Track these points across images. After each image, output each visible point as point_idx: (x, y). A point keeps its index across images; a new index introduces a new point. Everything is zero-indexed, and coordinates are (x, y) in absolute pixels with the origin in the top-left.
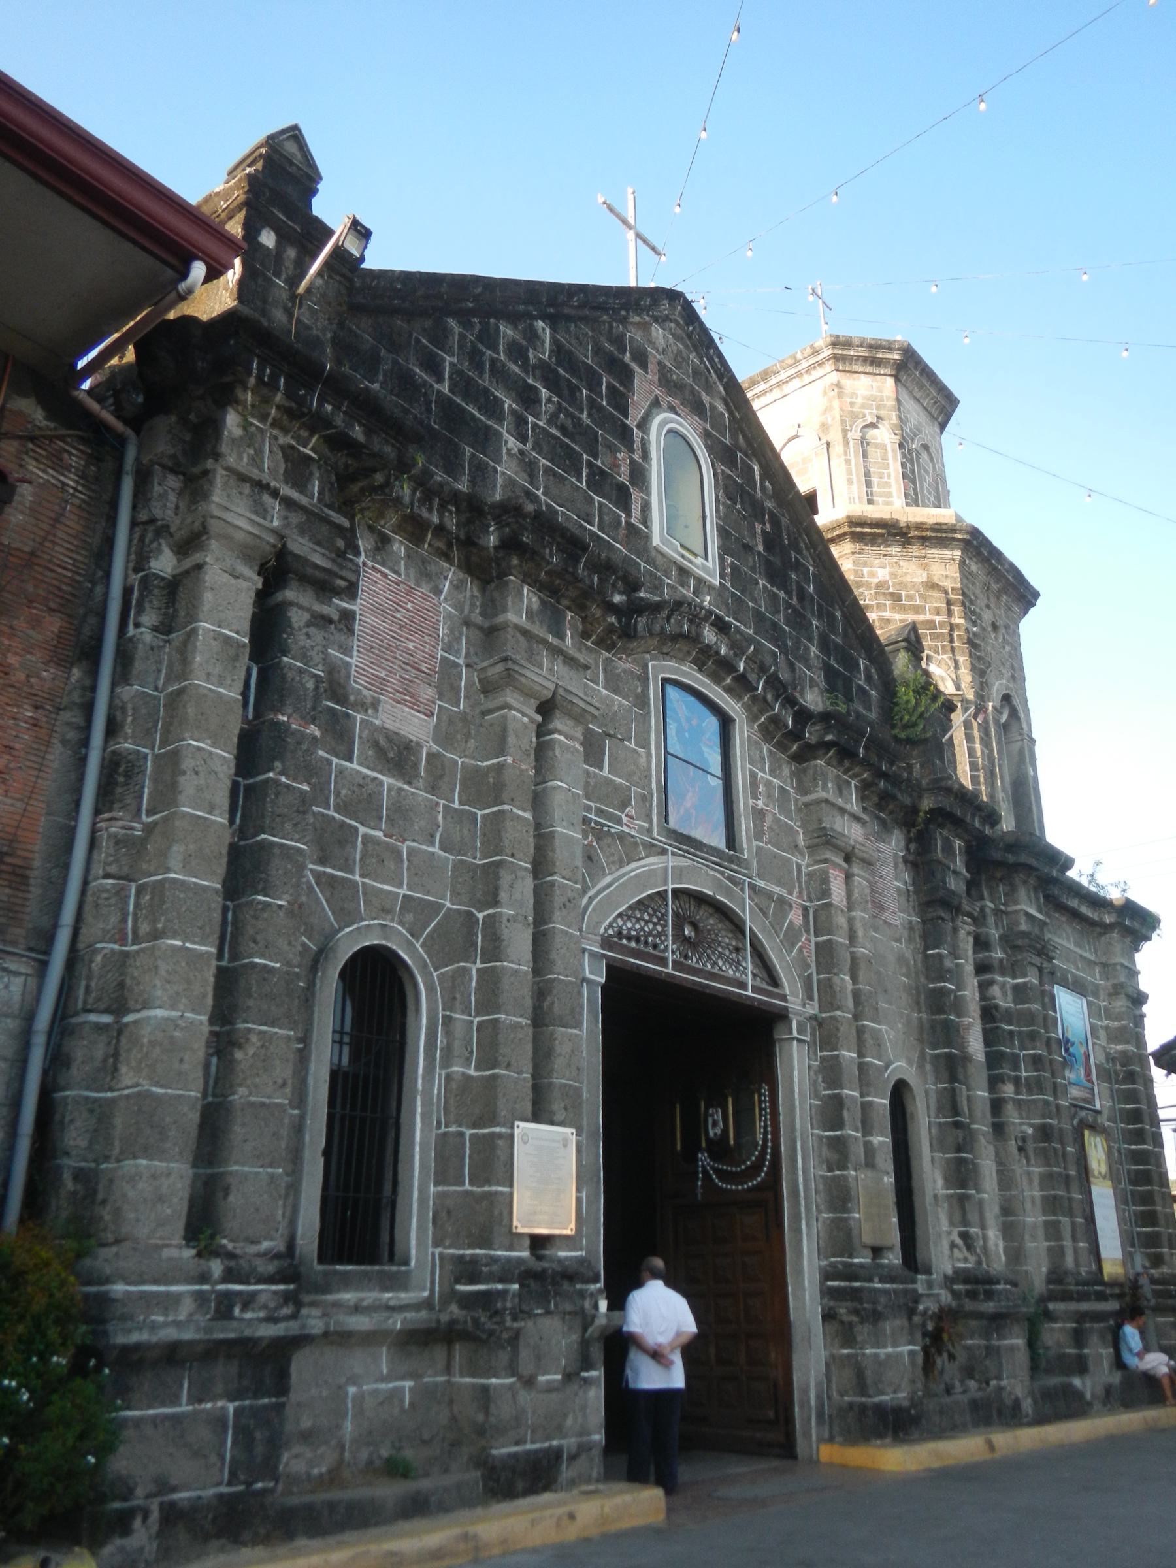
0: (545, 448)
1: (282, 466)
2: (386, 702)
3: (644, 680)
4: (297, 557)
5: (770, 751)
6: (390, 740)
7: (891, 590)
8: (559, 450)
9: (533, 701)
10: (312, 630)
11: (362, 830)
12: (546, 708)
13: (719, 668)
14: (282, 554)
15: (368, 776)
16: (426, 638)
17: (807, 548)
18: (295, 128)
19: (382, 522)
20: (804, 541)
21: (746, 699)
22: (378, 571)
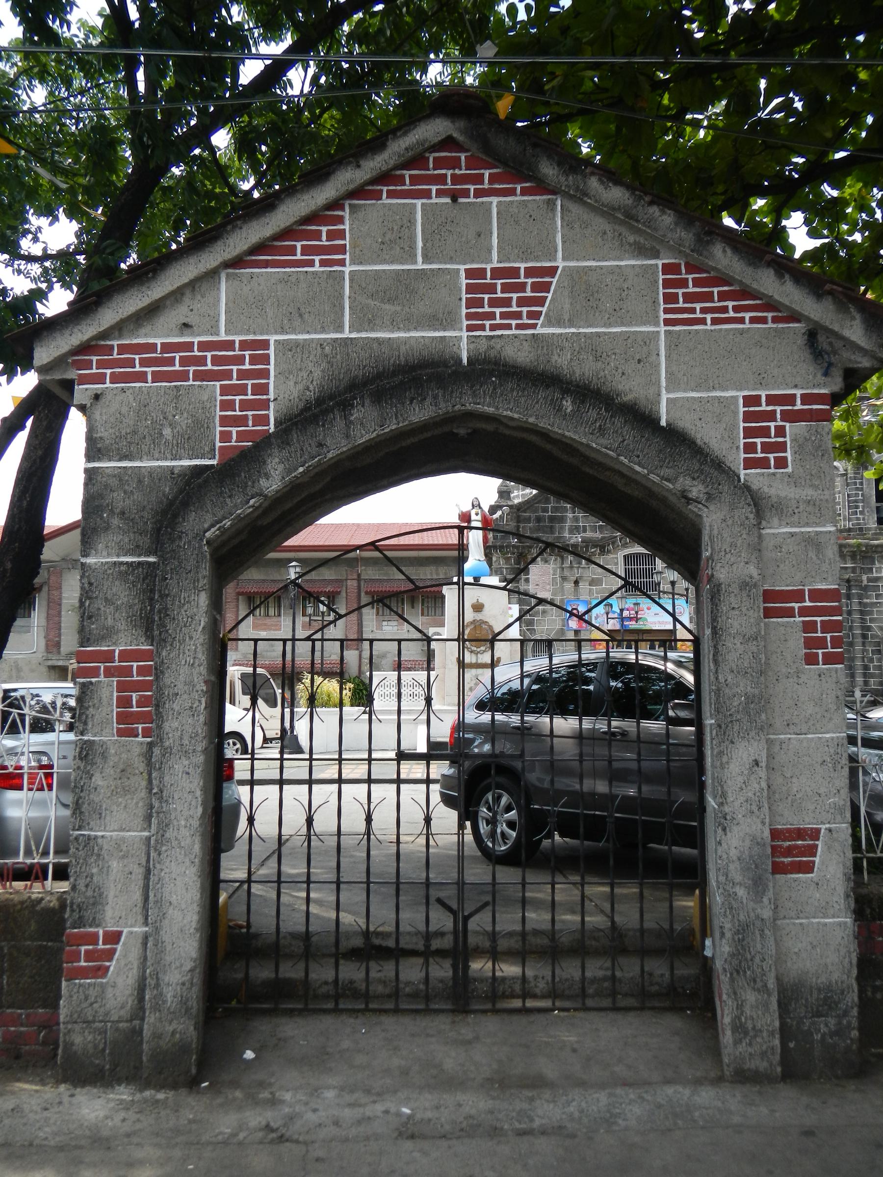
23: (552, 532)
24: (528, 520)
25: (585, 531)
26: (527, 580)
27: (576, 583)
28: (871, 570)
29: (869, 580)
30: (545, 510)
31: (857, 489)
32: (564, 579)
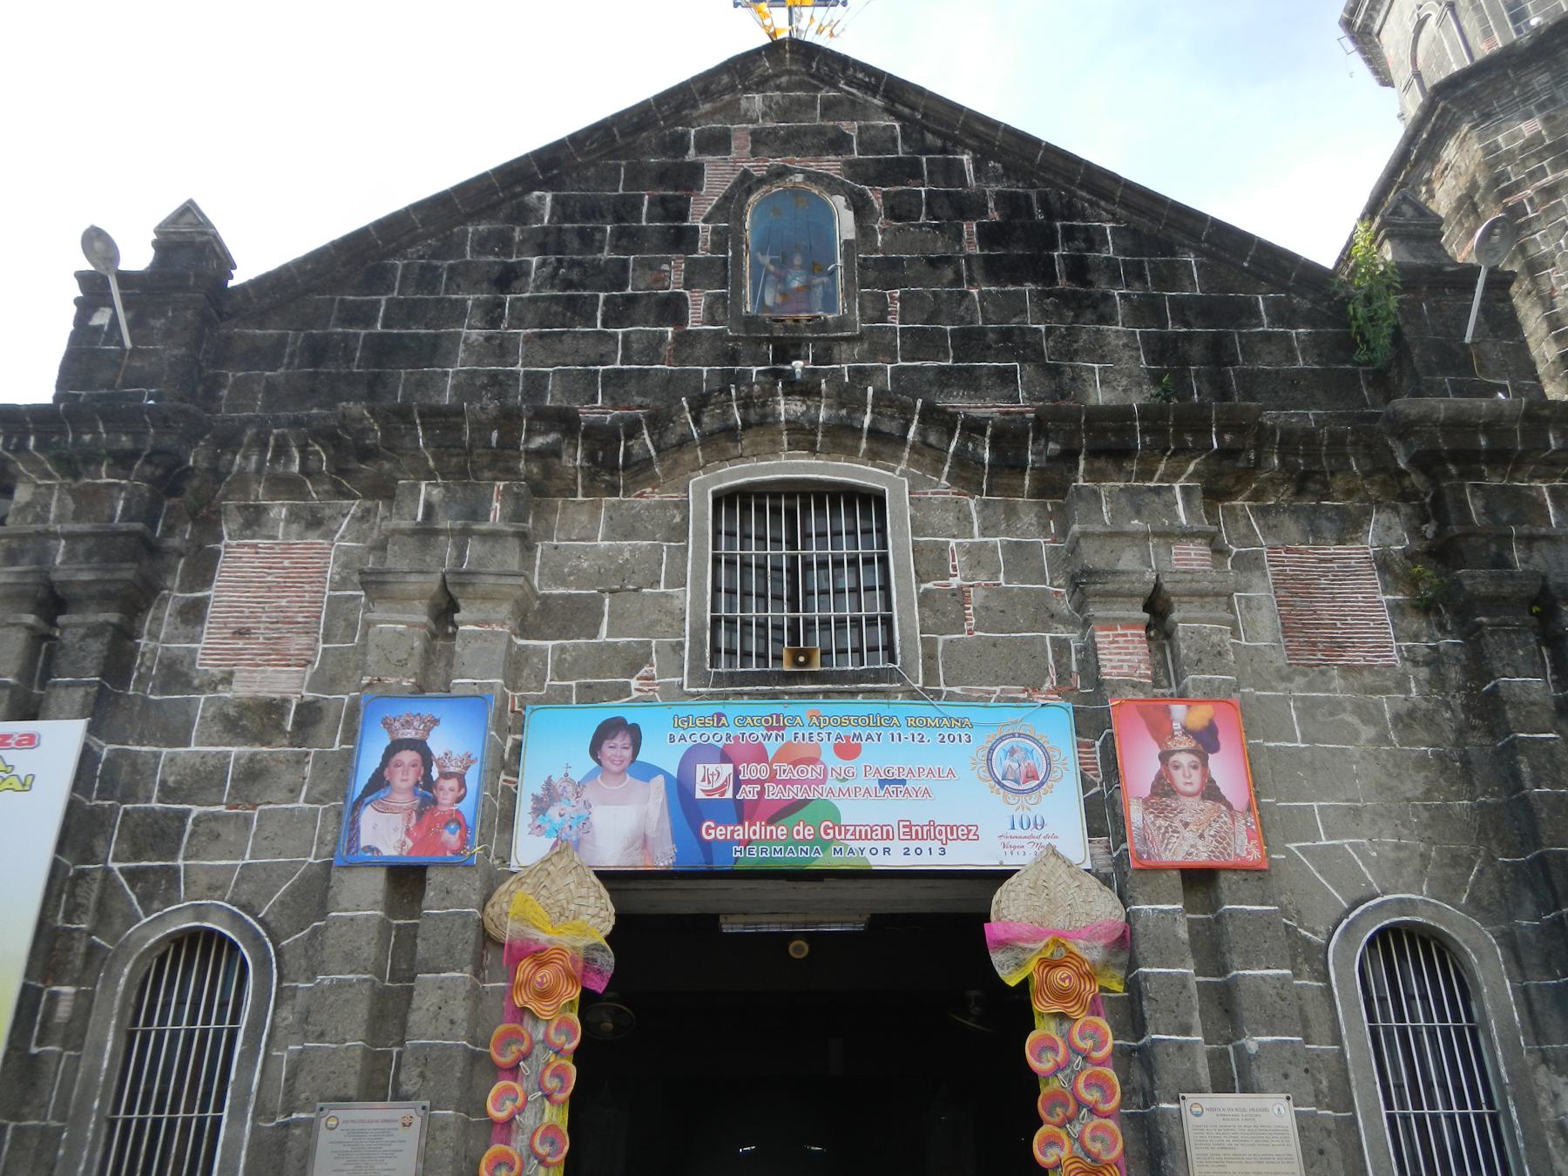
0: (529, 317)
1: (71, 506)
2: (241, 671)
3: (683, 506)
4: (64, 583)
5: (986, 504)
7: (1548, 142)
8: (554, 308)
9: (417, 602)
10: (90, 641)
11: (196, 810)
14: (50, 586)
15: (209, 752)
16: (307, 587)
17: (1092, 204)
18: (191, 202)
19: (252, 497)
20: (1082, 199)
21: (906, 455)
22: (244, 545)
24: (271, 355)
26: (193, 613)
30: (363, 316)
32: (375, 584)
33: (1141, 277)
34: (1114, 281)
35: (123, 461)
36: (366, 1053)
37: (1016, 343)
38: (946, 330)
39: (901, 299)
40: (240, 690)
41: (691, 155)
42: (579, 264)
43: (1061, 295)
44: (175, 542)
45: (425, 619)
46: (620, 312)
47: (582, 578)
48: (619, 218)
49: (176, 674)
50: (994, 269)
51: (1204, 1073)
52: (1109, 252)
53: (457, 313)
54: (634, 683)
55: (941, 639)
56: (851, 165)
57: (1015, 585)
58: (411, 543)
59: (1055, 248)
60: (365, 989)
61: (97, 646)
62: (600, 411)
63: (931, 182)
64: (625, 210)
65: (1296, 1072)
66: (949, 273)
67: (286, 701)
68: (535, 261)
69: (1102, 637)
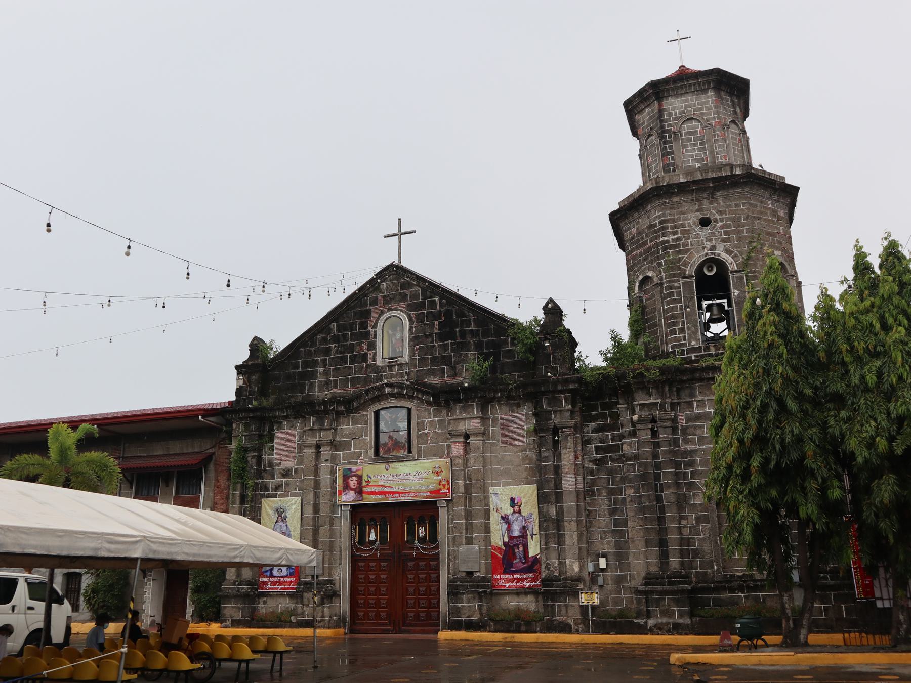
5: (434, 409)
6: (284, 470)
12: (318, 447)
13: (399, 396)
18: (255, 337)
23: (302, 391)
25: (335, 387)
26: (272, 448)
27: (318, 447)
28: (690, 404)
29: (689, 419)
31: (675, 301)
33: (479, 335)
34: (472, 338)
35: (251, 418)
36: (313, 542)
37: (446, 360)
38: (428, 358)
39: (419, 349)
40: (282, 466)
41: (368, 307)
42: (343, 346)
43: (458, 343)
44: (265, 433)
45: (314, 451)
46: (353, 360)
47: (346, 435)
48: (351, 331)
49: (271, 464)
50: (442, 337)
51: (464, 541)
52: (472, 327)
53: (315, 363)
54: (359, 461)
55: (423, 446)
56: (409, 305)
57: (440, 431)
58: (310, 432)
59: (457, 327)
60: (311, 530)
61: (254, 460)
62: (350, 390)
63: (428, 309)
64: (352, 327)
65: (481, 541)
66: (430, 340)
67: (292, 469)
68: (333, 345)
69: (453, 446)
